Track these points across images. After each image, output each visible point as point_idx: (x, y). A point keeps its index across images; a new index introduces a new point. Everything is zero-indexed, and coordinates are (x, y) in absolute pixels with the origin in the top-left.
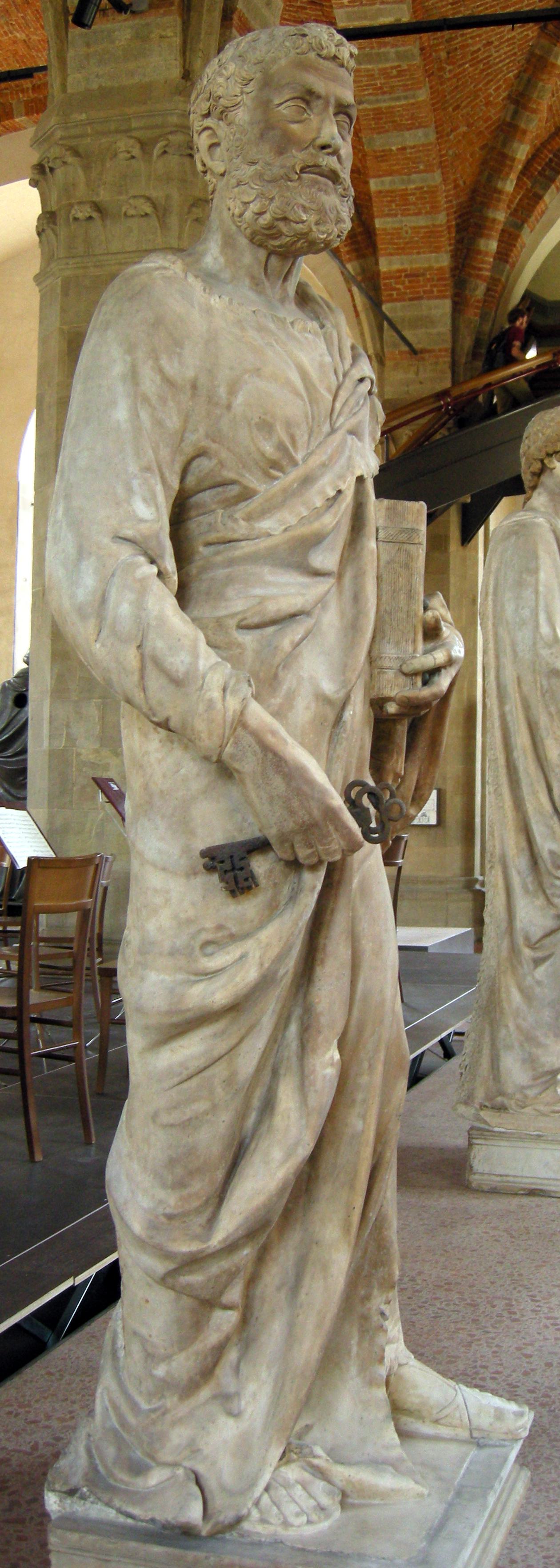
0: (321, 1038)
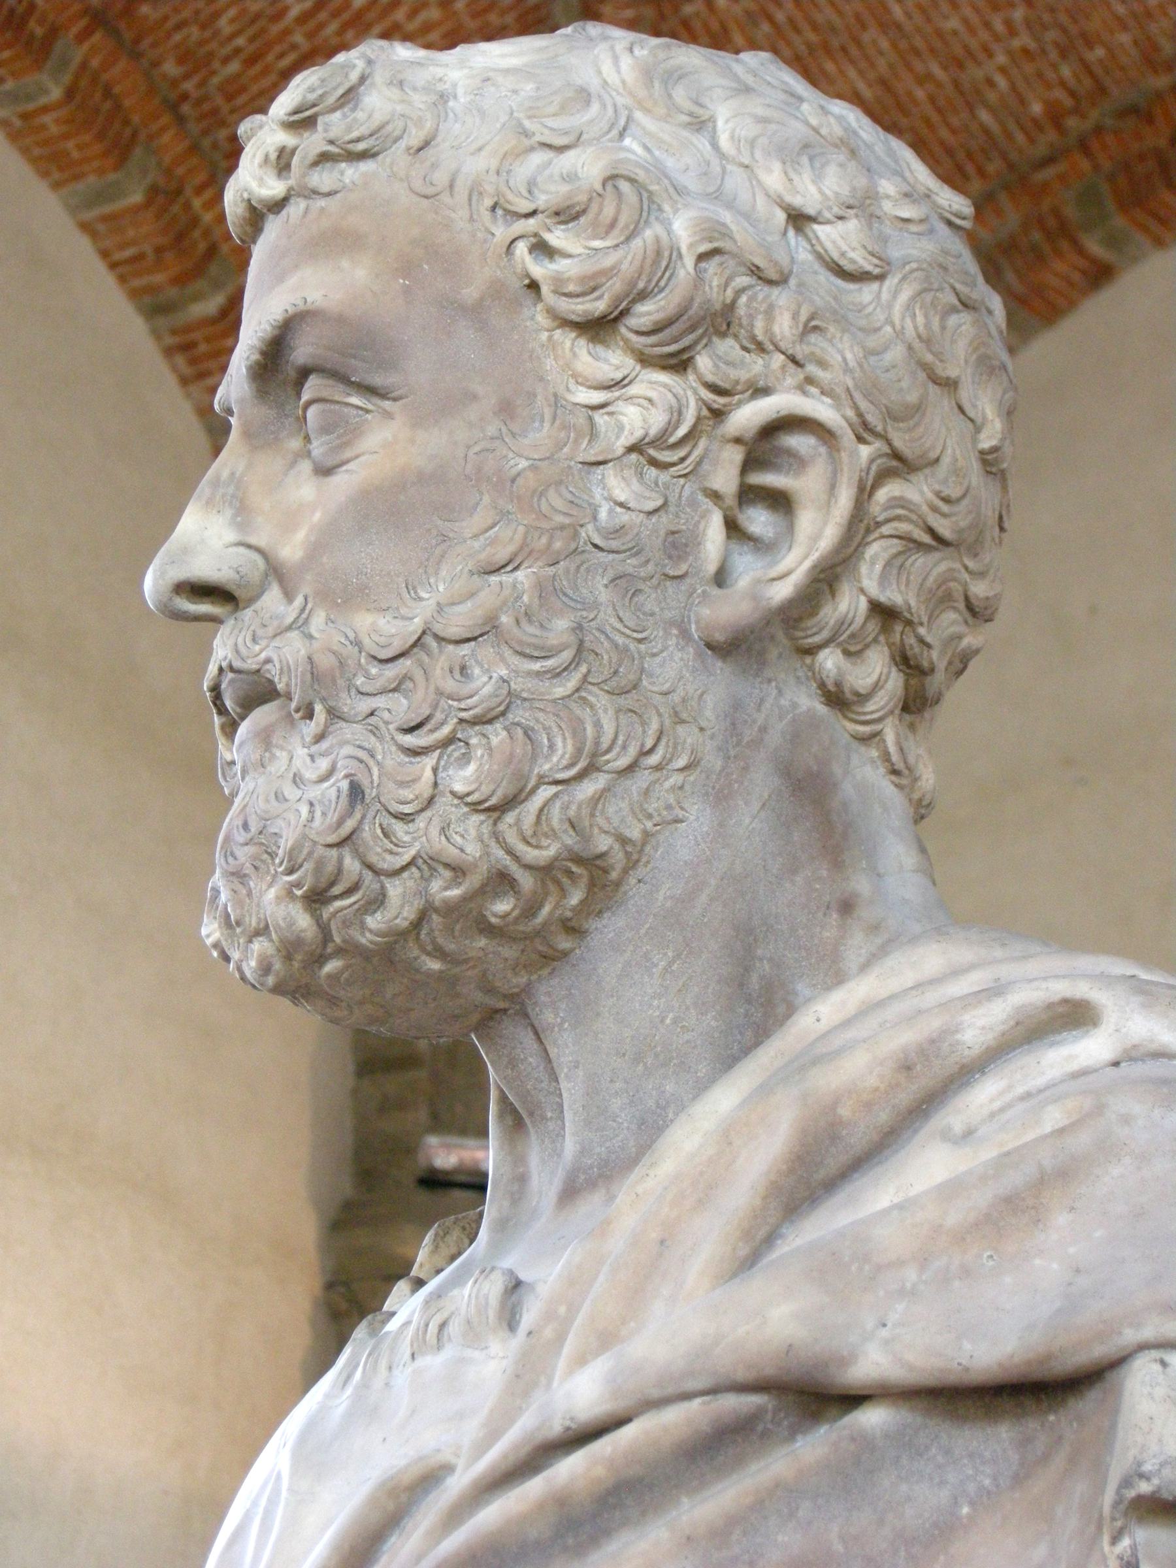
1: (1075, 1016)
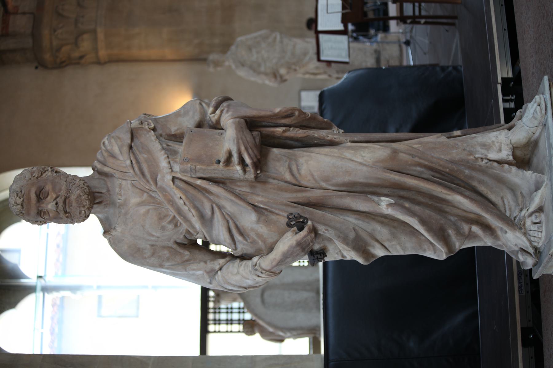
0: (378, 211)
1: (104, 143)
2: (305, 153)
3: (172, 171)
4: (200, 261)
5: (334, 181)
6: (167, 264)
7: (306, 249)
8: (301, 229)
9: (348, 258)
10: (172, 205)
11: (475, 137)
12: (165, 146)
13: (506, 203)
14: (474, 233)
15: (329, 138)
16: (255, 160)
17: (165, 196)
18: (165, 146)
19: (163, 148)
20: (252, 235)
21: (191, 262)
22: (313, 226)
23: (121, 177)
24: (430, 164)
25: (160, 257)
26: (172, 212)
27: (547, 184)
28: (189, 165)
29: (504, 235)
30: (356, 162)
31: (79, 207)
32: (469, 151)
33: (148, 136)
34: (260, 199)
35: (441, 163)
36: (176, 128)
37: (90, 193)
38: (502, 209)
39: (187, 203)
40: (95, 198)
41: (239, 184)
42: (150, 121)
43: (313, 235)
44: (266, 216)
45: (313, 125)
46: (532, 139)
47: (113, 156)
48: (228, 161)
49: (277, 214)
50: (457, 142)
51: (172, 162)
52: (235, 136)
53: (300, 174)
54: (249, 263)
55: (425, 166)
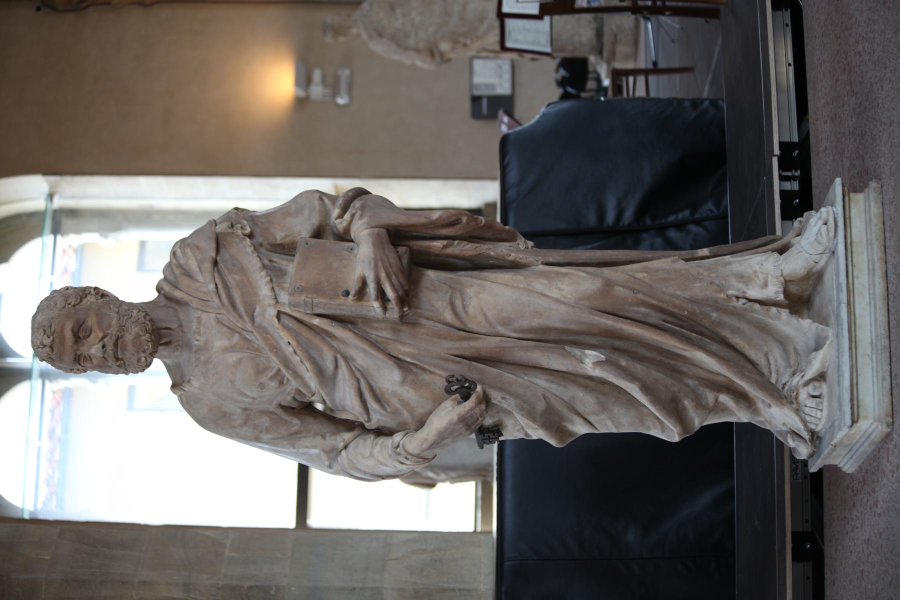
2: (475, 281)
3: (277, 302)
4: (316, 434)
5: (516, 325)
6: (266, 437)
7: (473, 427)
8: (466, 398)
9: (535, 437)
10: (276, 353)
11: (729, 263)
12: (266, 262)
13: (772, 361)
14: (723, 404)
15: (511, 258)
16: (401, 293)
17: (266, 339)
18: (266, 262)
19: (264, 267)
20: (394, 401)
21: (302, 435)
22: (484, 392)
23: (200, 307)
24: (661, 304)
25: (255, 426)
26: (276, 364)
27: (832, 342)
28: (303, 297)
29: (767, 409)
30: (550, 297)
31: (138, 352)
32: (718, 286)
33: (241, 245)
34: (406, 349)
35: (677, 302)
36: (283, 234)
37: (153, 331)
38: (765, 371)
39: (298, 352)
40: (160, 337)
41: (375, 325)
42: (245, 222)
43: (483, 406)
44: (415, 374)
45: (488, 235)
46: (815, 270)
47: (188, 275)
48: (361, 293)
49: (431, 373)
50: (701, 270)
51: (276, 289)
52: (372, 256)
53: (466, 312)
54: (389, 442)
55: (652, 306)
